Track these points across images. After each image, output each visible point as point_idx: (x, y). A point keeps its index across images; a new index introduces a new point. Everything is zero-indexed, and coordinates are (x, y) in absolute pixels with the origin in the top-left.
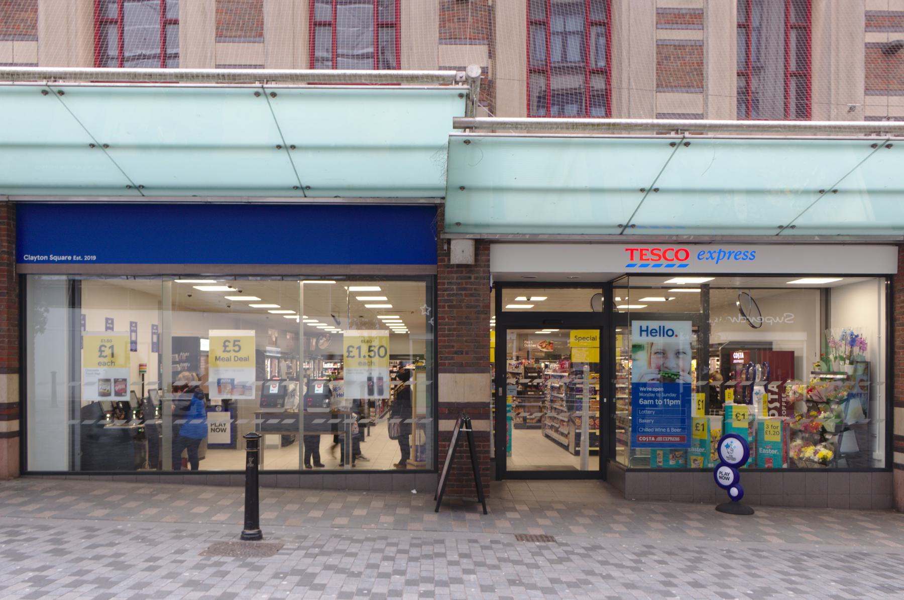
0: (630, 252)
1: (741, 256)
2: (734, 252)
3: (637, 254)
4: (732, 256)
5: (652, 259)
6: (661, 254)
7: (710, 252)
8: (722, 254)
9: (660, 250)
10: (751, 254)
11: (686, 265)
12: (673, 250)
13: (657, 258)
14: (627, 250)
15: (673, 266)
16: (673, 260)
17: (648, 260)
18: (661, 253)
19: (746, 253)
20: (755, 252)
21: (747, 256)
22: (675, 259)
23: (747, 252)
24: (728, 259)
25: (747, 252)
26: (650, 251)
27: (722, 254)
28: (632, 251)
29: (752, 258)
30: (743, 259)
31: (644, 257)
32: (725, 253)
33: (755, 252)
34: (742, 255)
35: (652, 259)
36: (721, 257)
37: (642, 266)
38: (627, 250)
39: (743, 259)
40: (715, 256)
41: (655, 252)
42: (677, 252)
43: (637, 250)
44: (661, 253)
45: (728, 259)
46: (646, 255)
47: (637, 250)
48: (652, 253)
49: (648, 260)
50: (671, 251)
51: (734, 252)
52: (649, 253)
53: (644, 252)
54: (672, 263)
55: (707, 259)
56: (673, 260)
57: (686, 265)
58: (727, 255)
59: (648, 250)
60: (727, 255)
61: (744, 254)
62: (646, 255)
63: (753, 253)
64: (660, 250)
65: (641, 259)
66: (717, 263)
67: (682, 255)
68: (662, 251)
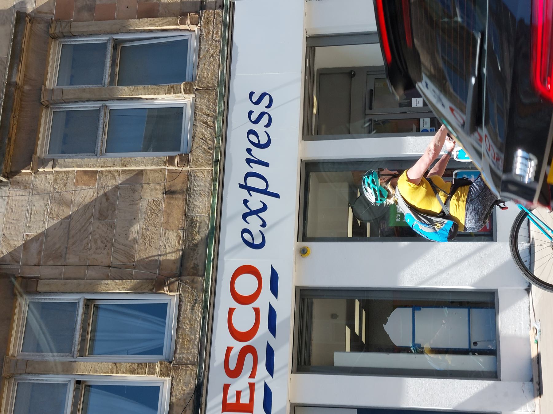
1: (259, 128)
2: (249, 151)
4: (258, 153)
6: (242, 345)
7: (245, 216)
8: (252, 182)
9: (229, 349)
10: (257, 103)
12: (231, 311)
16: (257, 311)
17: (252, 386)
18: (238, 346)
19: (254, 117)
20: (252, 94)
21: (262, 114)
22: (255, 304)
23: (250, 113)
24: (267, 165)
25: (250, 113)
26: (228, 380)
27: (252, 182)
29: (266, 100)
30: (268, 126)
31: (245, 399)
32: (248, 175)
33: (252, 94)
34: (257, 128)
36: (261, 185)
39: (268, 126)
40: (256, 200)
44: (238, 346)
45: (267, 165)
46: (238, 393)
49: (252, 386)
51: (249, 151)
55: (264, 225)
56: (257, 311)
58: (257, 168)
59: (226, 387)
60: (257, 168)
61: (256, 122)
62: (238, 393)
63: (255, 98)
64: (229, 349)
66: (277, 196)
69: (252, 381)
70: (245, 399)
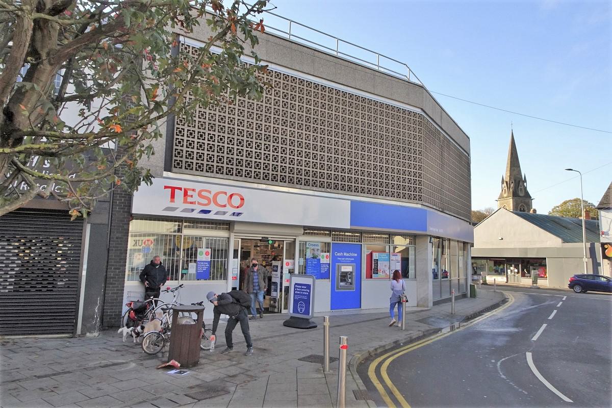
0: (170, 189)
3: (179, 194)
5: (199, 203)
9: (210, 192)
11: (239, 214)
12: (226, 193)
13: (206, 202)
14: (166, 187)
15: (224, 213)
16: (225, 206)
18: (211, 196)
22: (228, 206)
26: (197, 191)
28: (173, 189)
35: (199, 203)
37: (185, 210)
38: (166, 187)
41: (204, 193)
42: (231, 196)
43: (180, 189)
44: (211, 196)
46: (192, 196)
47: (180, 189)
48: (200, 195)
50: (223, 195)
52: (195, 195)
53: (190, 193)
54: (222, 209)
56: (225, 206)
57: (239, 214)
64: (210, 192)
65: (185, 201)
67: (236, 201)
68: (213, 193)
69: (197, 203)
70: (189, 199)
